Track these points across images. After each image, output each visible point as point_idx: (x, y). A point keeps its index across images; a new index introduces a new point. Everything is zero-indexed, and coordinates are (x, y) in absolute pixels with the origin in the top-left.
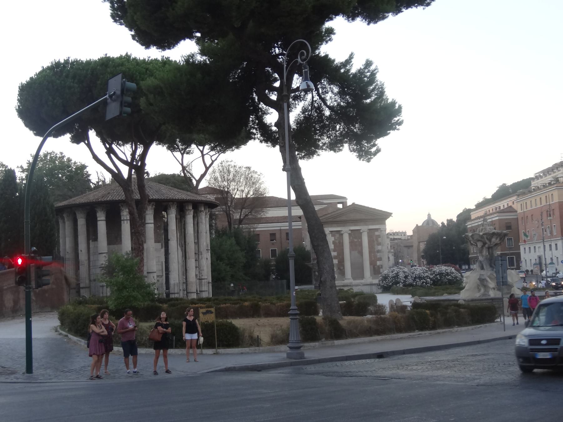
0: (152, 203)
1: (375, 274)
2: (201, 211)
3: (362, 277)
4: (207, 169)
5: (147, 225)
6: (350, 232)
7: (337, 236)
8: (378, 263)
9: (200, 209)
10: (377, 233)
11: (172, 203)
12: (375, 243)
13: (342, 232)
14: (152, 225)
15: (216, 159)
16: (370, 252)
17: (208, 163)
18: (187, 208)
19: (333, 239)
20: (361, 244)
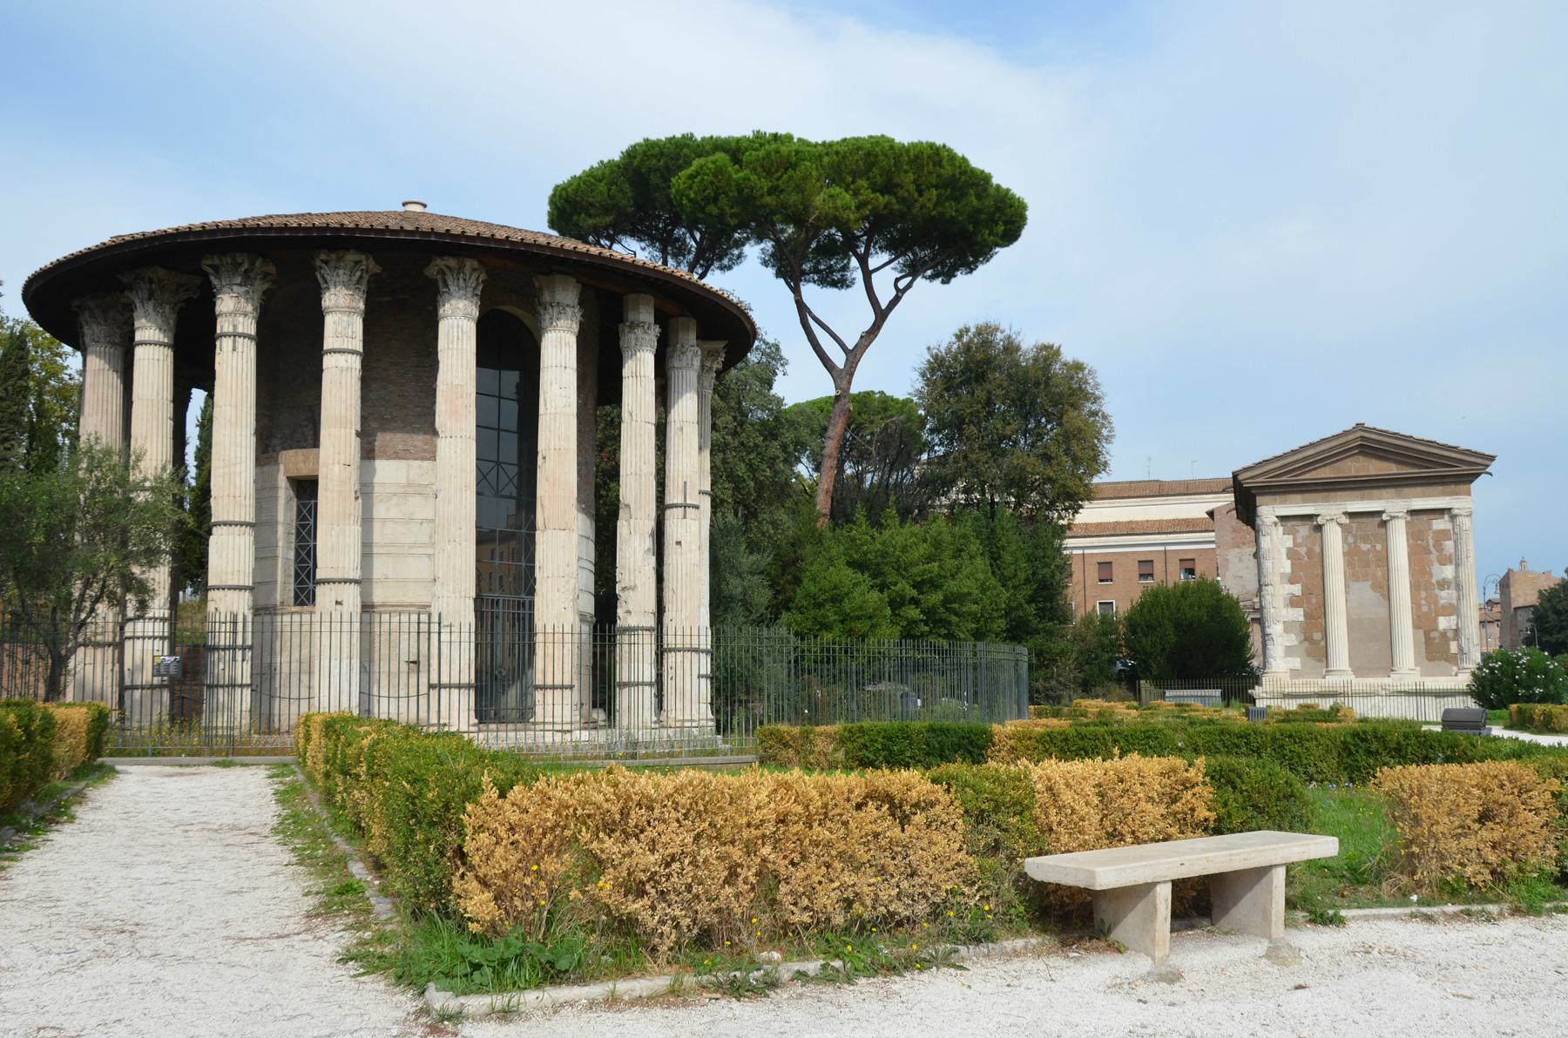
0: (351, 257)
1: (1430, 658)
2: (634, 326)
3: (1389, 667)
4: (881, 315)
5: (328, 361)
6: (1345, 520)
7: (1304, 530)
8: (1444, 623)
9: (631, 316)
10: (1440, 524)
11: (452, 262)
12: (1434, 555)
13: (1320, 520)
14: (355, 362)
15: (909, 286)
16: (1415, 587)
17: (885, 295)
18: (546, 297)
19: (1288, 541)
20: (1384, 560)
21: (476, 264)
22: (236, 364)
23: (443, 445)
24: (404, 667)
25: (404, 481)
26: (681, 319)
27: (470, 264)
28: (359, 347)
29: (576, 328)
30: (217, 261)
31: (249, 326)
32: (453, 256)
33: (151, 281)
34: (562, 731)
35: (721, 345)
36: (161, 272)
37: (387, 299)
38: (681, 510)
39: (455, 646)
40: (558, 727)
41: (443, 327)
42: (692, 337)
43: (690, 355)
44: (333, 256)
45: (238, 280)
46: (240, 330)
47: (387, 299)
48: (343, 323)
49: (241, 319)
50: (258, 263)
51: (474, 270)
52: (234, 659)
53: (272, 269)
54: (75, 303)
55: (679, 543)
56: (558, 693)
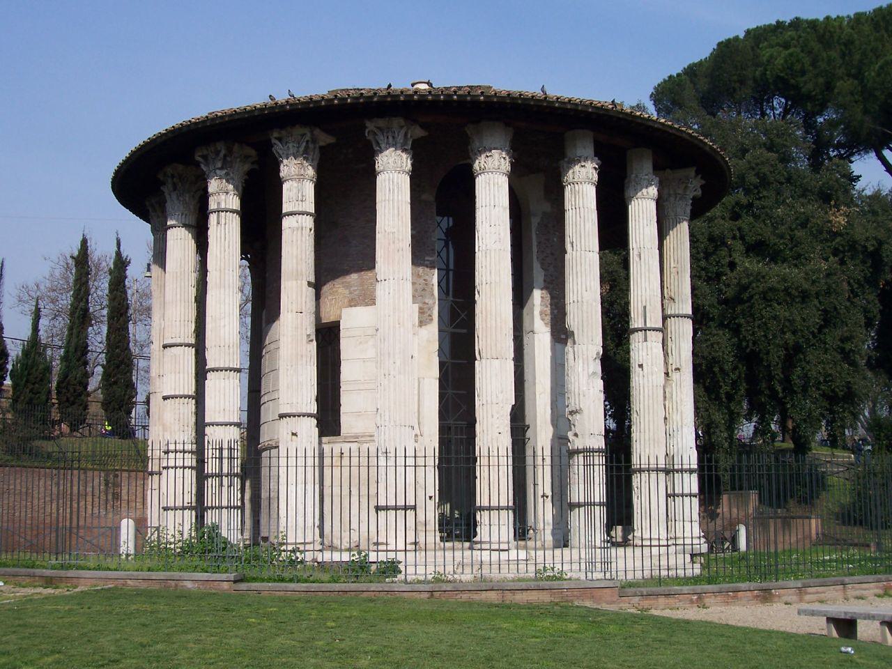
0: (298, 130)
5: (287, 223)
9: (569, 154)
11: (381, 123)
14: (309, 222)
21: (402, 121)
22: (226, 233)
23: (381, 291)
27: (397, 122)
28: (311, 208)
29: (506, 166)
30: (205, 152)
31: (234, 202)
33: (173, 176)
34: (499, 550)
35: (691, 172)
36: (181, 167)
38: (640, 335)
39: (391, 471)
40: (495, 546)
41: (381, 181)
42: (648, 166)
44: (284, 132)
45: (219, 165)
46: (223, 206)
48: (298, 189)
49: (223, 197)
51: (402, 127)
52: (221, 485)
53: (253, 152)
54: (147, 203)
55: (641, 366)
56: (494, 513)
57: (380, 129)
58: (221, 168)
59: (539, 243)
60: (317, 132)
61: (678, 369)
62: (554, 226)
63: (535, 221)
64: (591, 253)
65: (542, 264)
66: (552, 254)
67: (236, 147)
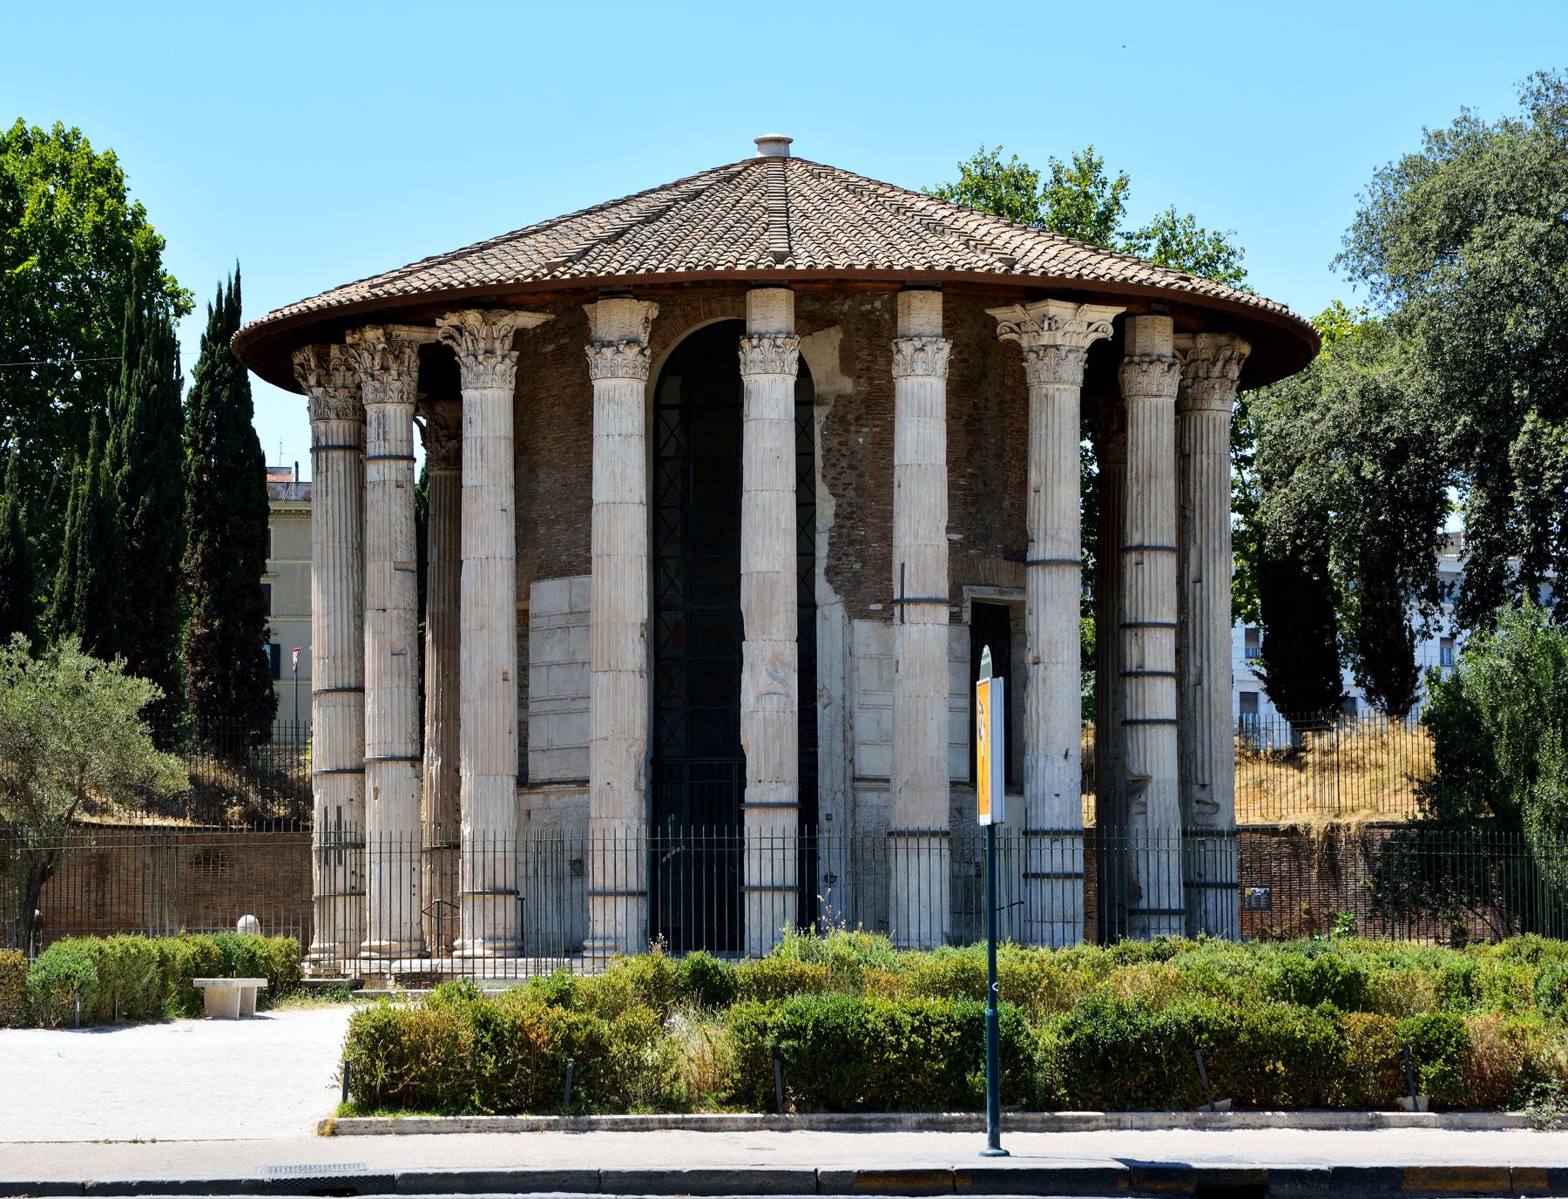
11: (453, 319)
24: (567, 868)
25: (566, 609)
26: (901, 296)
27: (472, 318)
32: (454, 311)
37: (551, 348)
43: (907, 348)
45: (312, 380)
47: (551, 348)
50: (335, 351)
57: (459, 330)
58: (319, 384)
59: (828, 451)
60: (402, 332)
61: (1036, 663)
62: (858, 419)
63: (820, 414)
64: (766, 495)
65: (832, 487)
66: (851, 467)
67: (335, 351)
